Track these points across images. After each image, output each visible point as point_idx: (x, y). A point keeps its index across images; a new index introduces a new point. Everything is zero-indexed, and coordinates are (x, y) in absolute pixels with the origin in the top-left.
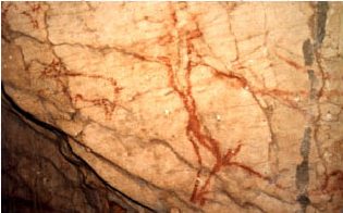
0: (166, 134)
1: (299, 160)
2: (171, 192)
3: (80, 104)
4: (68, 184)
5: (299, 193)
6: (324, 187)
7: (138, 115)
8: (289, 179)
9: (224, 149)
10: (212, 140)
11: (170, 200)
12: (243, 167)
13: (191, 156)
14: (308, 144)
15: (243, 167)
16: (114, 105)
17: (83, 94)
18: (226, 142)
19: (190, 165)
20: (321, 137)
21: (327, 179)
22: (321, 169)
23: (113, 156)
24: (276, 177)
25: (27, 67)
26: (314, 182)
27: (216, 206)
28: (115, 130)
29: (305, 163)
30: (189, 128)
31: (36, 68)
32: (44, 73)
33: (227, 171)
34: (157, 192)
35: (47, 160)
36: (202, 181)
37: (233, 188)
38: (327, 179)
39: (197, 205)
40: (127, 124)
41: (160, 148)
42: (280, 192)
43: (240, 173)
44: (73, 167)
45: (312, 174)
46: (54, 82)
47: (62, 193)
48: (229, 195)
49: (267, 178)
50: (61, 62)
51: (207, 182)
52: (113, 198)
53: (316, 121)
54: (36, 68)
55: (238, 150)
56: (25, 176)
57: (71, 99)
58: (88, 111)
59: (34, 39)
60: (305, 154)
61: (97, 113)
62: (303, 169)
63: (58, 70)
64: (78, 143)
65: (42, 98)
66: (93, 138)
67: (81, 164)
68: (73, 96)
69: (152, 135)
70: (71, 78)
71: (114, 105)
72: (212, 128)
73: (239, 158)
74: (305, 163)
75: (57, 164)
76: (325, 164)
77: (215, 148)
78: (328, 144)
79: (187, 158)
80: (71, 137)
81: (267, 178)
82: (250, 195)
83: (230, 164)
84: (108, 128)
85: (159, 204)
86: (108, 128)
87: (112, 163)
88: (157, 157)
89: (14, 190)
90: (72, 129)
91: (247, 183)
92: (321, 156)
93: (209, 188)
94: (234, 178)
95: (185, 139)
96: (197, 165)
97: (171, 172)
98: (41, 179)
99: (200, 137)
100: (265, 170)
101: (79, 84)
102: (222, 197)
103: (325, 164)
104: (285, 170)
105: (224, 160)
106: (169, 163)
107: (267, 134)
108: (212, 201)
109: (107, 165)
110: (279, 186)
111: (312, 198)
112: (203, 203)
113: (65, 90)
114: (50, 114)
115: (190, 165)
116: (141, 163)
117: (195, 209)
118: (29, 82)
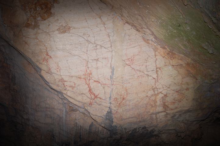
0: (84, 92)
1: (110, 96)
2: (85, 103)
3: (67, 87)
4: (59, 103)
5: (110, 102)
6: (114, 100)
7: (79, 89)
8: (108, 99)
9: (96, 95)
10: (93, 93)
11: (85, 105)
12: (99, 98)
13: (89, 96)
14: (111, 93)
15: (99, 98)
16: (74, 87)
17: (67, 85)
18: (96, 94)
19: (89, 98)
20: (113, 92)
21: (114, 99)
22: (113, 97)
23: (73, 97)
24: (106, 99)
25: (55, 80)
26: (112, 99)
27: (94, 105)
28: (74, 92)
29: (111, 96)
30: (89, 91)
31: (57, 80)
32: (59, 81)
33: (96, 99)
34: (82, 103)
35: (54, 98)
36: (91, 101)
37: (98, 102)
38: (114, 99)
39: (90, 105)
40: (77, 91)
41: (83, 95)
42: (106, 102)
43: (99, 99)
44: (60, 99)
45: (112, 98)
46: (61, 83)
47: (57, 105)
48: (97, 103)
49: (104, 100)
50: (63, 79)
51: (93, 101)
52: (70, 105)
53: (112, 89)
54: (57, 80)
55: (98, 95)
56: (49, 102)
57: (65, 86)
58: (68, 88)
59: (57, 74)
60: (111, 95)
61: (70, 89)
62: (110, 98)
63: (62, 80)
64: (66, 95)
65: (58, 86)
66: (69, 94)
67: (65, 98)
68: (65, 85)
69: (82, 93)
70: (65, 82)
71: (74, 87)
72: (93, 91)
73: (98, 96)
74: (111, 96)
75: (57, 99)
76: (114, 96)
77: (94, 95)
78: (115, 93)
79: (88, 96)
80: (64, 94)
81: (104, 100)
82: (100, 103)
83: (97, 97)
84: (72, 92)
85: (82, 106)
86: (72, 92)
87: (73, 98)
88: (83, 97)
89: (45, 105)
90: (64, 92)
91: (100, 101)
92: (113, 95)
93: (93, 102)
94: (98, 100)
95: (88, 93)
96: (90, 98)
97: (86, 99)
98: (52, 102)
99: (91, 93)
100: (103, 98)
101: (67, 83)
102: (96, 104)
103: (114, 96)
104: (107, 98)
105: (96, 97)
106: (85, 98)
107: (104, 92)
108: (93, 105)
109: (72, 99)
110: (106, 101)
111: (112, 103)
112: (91, 105)
113: (64, 84)
114: (60, 89)
115: (89, 98)
116: (79, 98)
117: (90, 106)
118: (55, 83)
